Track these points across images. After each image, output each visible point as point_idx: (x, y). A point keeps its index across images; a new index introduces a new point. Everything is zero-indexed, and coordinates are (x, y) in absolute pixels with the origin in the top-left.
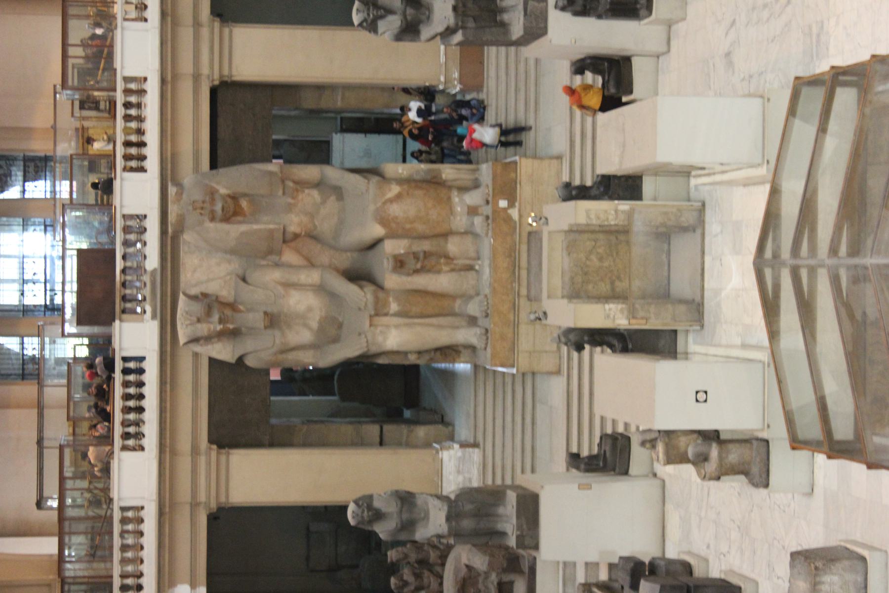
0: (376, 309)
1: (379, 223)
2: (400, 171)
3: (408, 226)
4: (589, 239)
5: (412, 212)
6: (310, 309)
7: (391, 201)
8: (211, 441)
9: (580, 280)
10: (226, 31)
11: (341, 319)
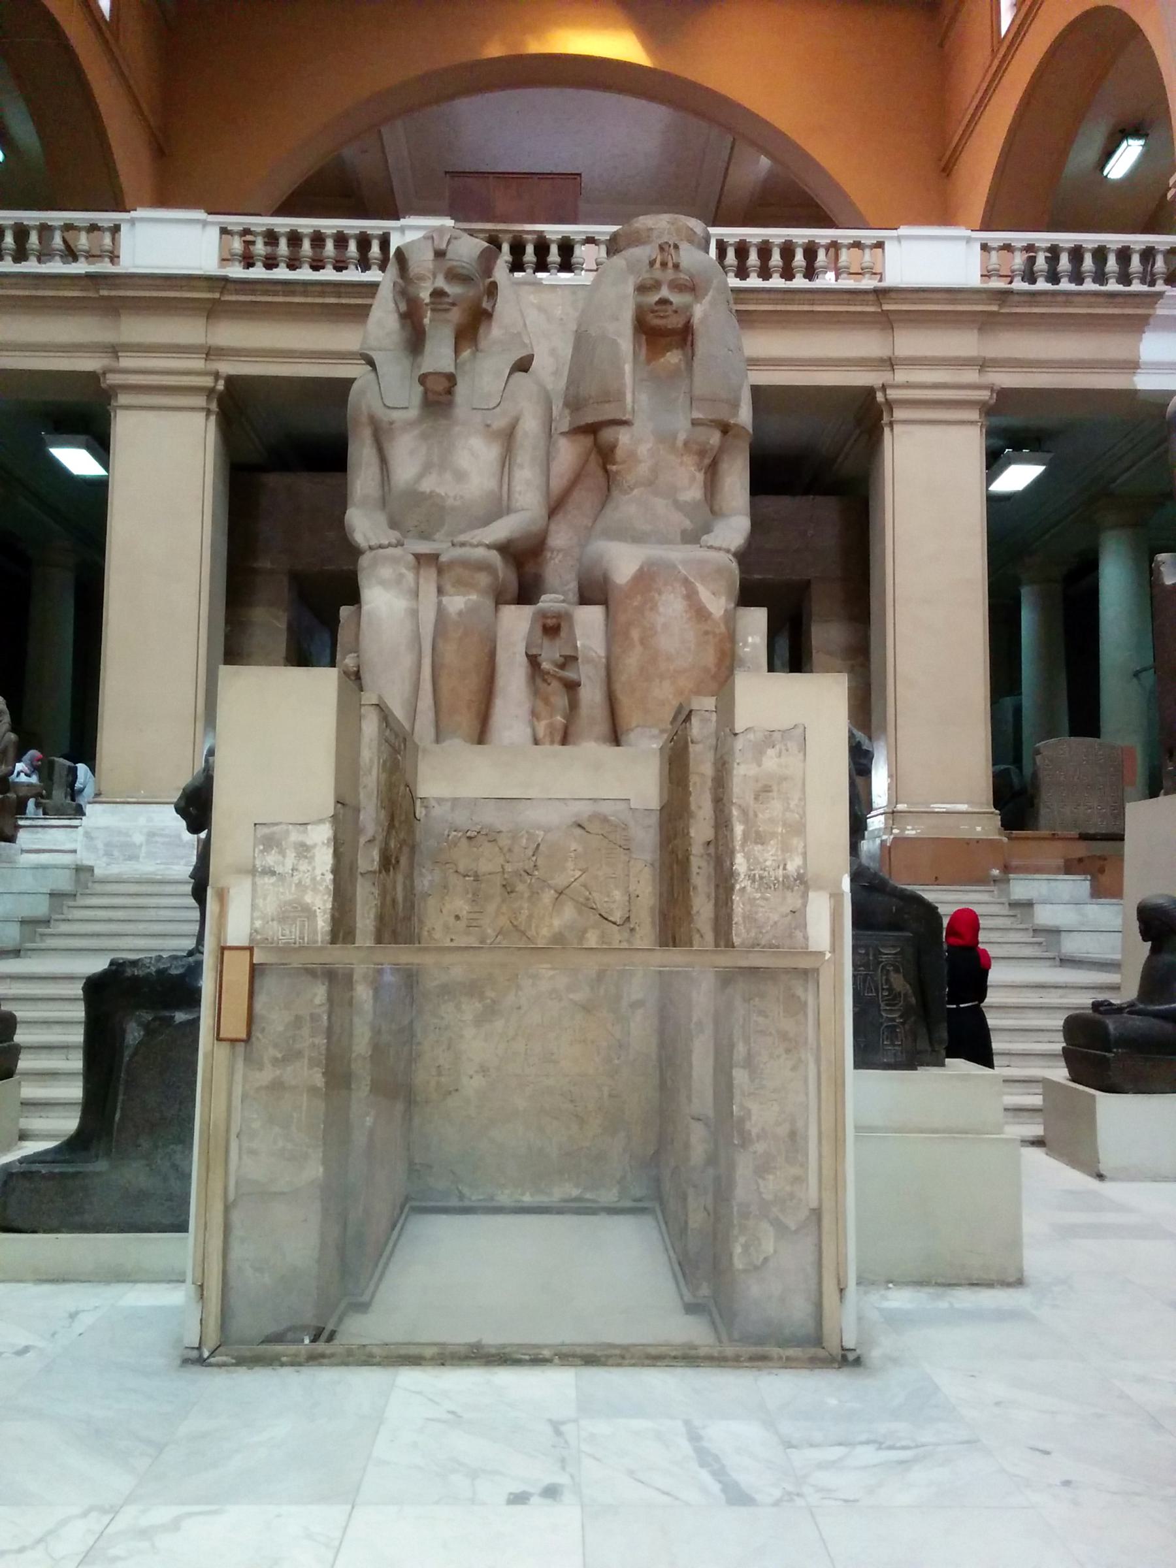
0: (452, 564)
1: (641, 570)
2: (750, 640)
3: (635, 634)
4: (631, 898)
5: (667, 643)
6: (461, 476)
7: (691, 596)
8: (231, 380)
9: (484, 867)
10: (974, 415)
11: (437, 536)
